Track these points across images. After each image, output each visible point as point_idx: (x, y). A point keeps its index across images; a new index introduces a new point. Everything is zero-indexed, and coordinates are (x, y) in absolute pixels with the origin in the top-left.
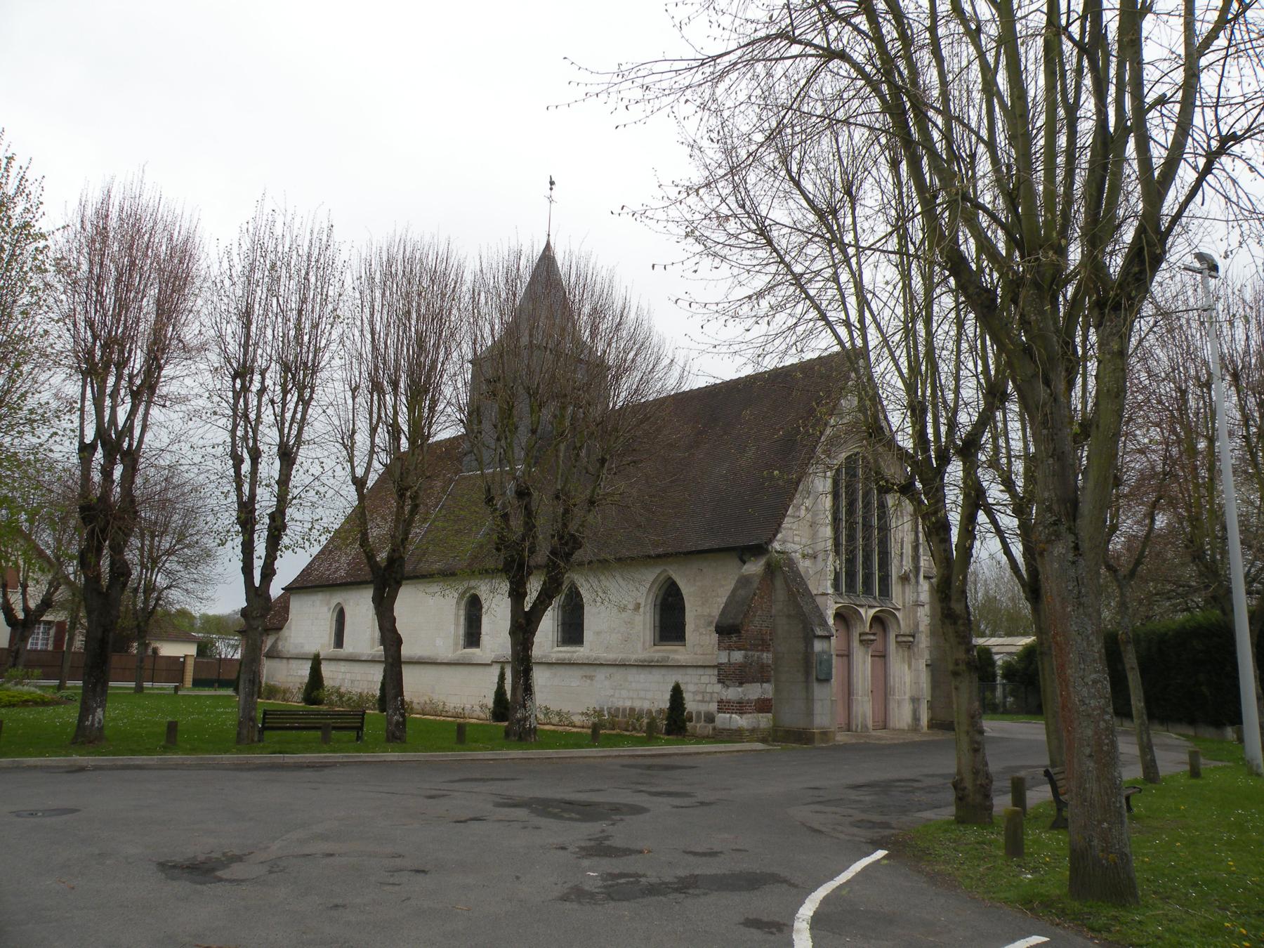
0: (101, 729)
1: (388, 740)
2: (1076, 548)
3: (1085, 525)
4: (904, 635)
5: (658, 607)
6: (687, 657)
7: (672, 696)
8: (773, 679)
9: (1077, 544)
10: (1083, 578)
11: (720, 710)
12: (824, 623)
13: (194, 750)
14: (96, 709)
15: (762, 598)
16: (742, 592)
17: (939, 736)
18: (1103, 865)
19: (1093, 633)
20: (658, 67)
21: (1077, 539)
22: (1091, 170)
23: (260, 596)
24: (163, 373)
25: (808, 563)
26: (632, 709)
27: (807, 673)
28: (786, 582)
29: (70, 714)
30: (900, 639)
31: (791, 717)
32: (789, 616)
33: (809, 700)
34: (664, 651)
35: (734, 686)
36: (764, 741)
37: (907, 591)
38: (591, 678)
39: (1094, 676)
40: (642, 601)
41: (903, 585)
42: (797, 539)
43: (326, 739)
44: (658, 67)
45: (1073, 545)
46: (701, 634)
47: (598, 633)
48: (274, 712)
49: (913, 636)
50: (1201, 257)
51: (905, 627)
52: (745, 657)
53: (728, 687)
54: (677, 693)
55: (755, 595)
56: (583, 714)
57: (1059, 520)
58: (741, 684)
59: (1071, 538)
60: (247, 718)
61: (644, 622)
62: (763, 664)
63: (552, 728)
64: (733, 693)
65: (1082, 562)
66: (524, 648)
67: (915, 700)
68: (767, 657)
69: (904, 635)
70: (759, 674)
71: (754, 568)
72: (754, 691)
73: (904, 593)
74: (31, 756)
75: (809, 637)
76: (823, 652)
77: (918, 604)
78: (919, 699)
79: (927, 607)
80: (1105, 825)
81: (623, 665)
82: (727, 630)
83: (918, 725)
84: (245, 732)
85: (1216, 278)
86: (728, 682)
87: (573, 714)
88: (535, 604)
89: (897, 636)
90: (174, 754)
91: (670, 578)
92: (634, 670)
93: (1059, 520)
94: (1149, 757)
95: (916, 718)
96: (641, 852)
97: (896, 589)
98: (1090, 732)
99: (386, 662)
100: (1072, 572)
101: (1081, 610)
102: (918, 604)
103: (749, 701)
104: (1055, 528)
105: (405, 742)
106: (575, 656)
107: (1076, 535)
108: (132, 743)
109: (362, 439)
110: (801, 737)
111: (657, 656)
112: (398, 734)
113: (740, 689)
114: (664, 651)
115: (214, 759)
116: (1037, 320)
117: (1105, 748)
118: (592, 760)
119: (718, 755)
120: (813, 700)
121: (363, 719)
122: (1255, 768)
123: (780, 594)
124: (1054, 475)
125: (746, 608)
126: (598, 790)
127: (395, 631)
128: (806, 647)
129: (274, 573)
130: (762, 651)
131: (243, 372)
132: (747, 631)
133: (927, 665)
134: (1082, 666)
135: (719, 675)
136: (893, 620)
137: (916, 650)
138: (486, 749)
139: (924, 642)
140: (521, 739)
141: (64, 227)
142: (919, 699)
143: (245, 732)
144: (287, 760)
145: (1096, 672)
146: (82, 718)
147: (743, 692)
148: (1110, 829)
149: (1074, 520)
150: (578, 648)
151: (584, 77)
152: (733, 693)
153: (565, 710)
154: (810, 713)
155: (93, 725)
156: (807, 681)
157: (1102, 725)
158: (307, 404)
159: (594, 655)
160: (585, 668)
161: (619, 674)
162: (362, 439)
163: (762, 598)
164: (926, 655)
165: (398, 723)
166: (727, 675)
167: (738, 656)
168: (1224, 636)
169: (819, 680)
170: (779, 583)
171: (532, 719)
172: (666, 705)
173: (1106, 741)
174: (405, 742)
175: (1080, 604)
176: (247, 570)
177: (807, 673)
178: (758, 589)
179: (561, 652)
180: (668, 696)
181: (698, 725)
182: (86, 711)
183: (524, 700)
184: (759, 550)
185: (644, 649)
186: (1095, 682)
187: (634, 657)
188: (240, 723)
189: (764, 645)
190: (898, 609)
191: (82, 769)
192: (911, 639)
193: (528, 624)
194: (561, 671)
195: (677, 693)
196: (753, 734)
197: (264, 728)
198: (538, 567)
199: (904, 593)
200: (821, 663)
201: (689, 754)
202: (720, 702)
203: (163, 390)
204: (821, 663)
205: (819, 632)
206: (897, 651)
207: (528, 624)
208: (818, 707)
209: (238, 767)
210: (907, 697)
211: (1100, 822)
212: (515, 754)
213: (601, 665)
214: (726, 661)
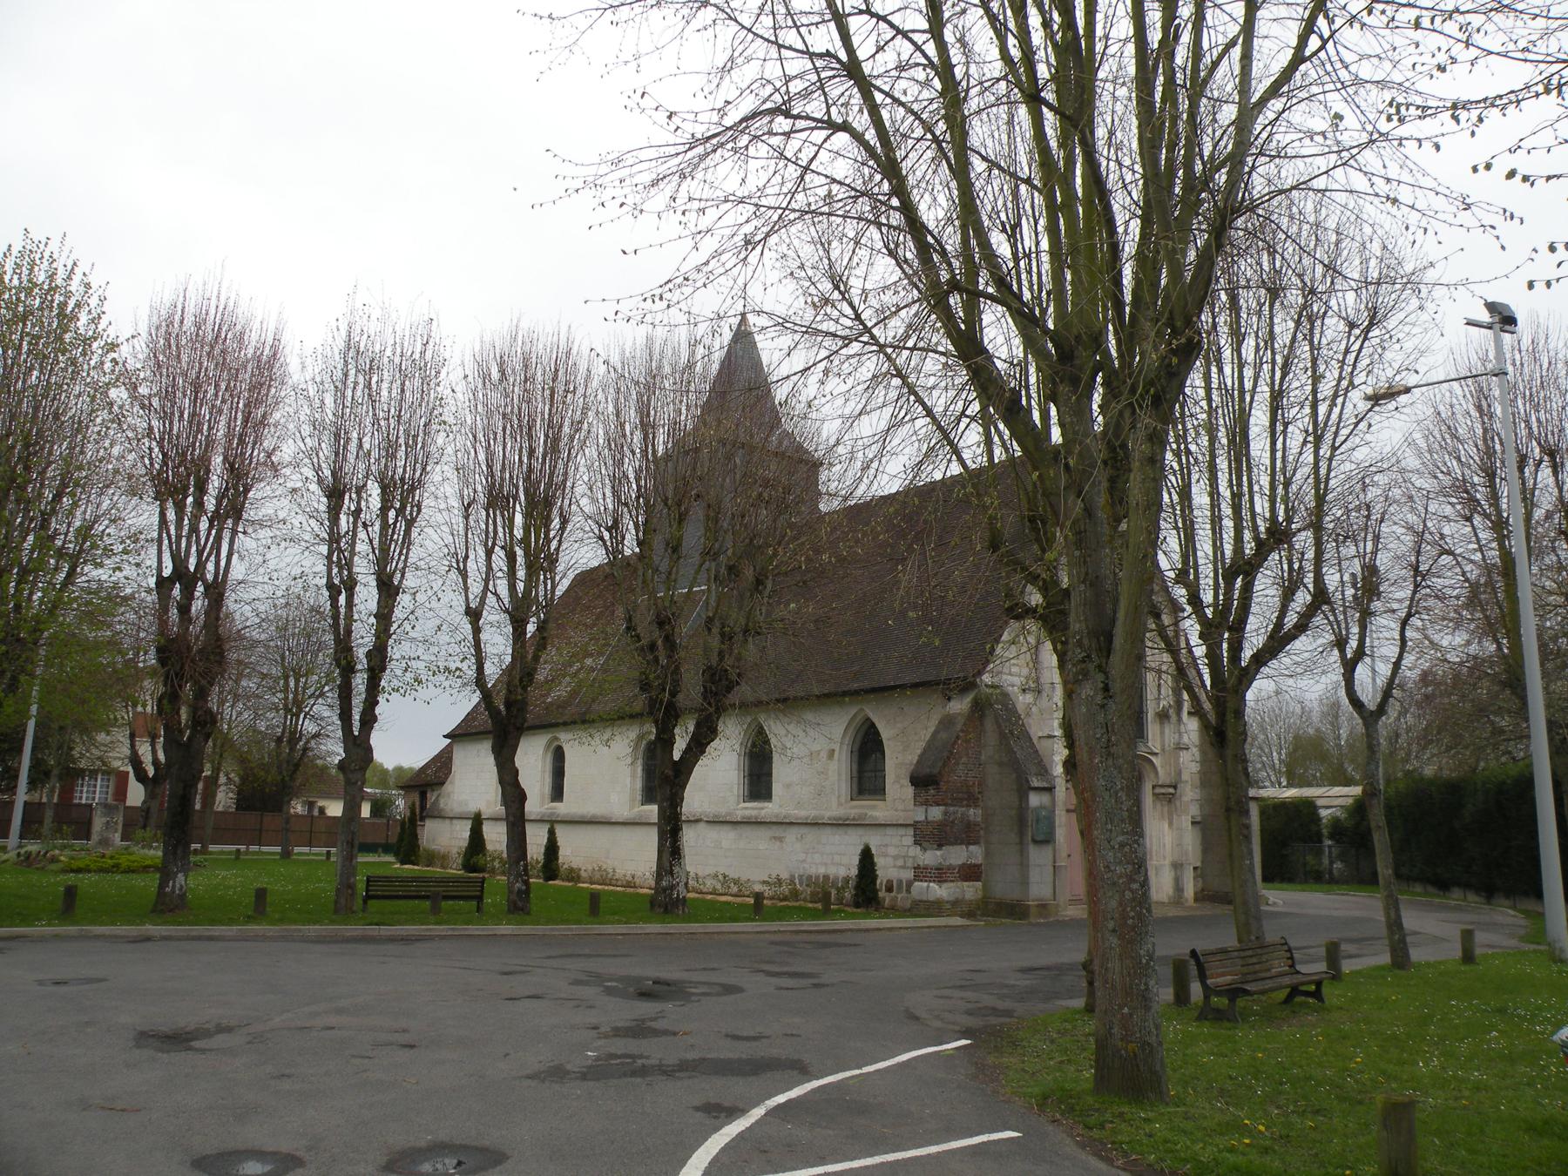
0: (183, 896)
1: (510, 911)
2: (1106, 689)
3: (1117, 662)
4: (1162, 786)
5: (856, 754)
6: (886, 813)
7: (860, 861)
8: (982, 841)
9: (1107, 685)
10: (1113, 724)
11: (917, 878)
12: (1044, 771)
13: (281, 921)
14: (177, 873)
15: (968, 741)
16: (943, 735)
17: (1208, 909)
18: (1121, 1056)
19: (1122, 789)
20: (644, 155)
21: (1107, 678)
22: (1052, 262)
23: (359, 745)
24: (251, 495)
25: (1029, 698)
26: (826, 877)
27: (1021, 834)
28: (997, 722)
29: (151, 882)
30: (1158, 790)
31: (1004, 888)
32: (1001, 764)
33: (1024, 866)
34: (862, 807)
35: (932, 849)
36: (970, 915)
37: (1167, 731)
38: (780, 839)
39: (1120, 838)
40: (837, 747)
41: (1162, 723)
42: (1014, 669)
43: (435, 910)
44: (644, 155)
45: (1102, 685)
46: (902, 786)
47: (788, 786)
48: (379, 879)
49: (1175, 787)
50: (1492, 307)
51: (1163, 775)
52: (945, 813)
53: (925, 850)
54: (867, 857)
55: (958, 738)
56: (764, 882)
57: (1088, 656)
58: (940, 846)
59: (1100, 677)
60: (346, 887)
61: (839, 771)
62: (969, 822)
63: (729, 898)
64: (931, 857)
65: (1112, 706)
66: (671, 804)
67: (1177, 866)
68: (974, 814)
69: (1162, 786)
70: (967, 834)
71: (960, 706)
72: (957, 855)
73: (1162, 733)
74: (102, 924)
75: (1024, 789)
76: (1042, 807)
77: (1180, 747)
78: (1182, 865)
79: (1195, 750)
80: (1126, 1010)
81: (815, 824)
82: (922, 781)
83: (1180, 897)
84: (343, 901)
85: (1513, 333)
86: (924, 844)
87: (754, 882)
88: (685, 752)
89: (1154, 787)
90: (259, 924)
91: (868, 719)
92: (828, 830)
93: (1088, 656)
94: (1397, 937)
95: (1179, 889)
96: (675, 1034)
97: (1152, 729)
98: (1114, 904)
99: (507, 819)
100: (1101, 718)
101: (1110, 762)
102: (1180, 747)
103: (950, 867)
104: (1083, 666)
105: (528, 913)
106: (763, 812)
107: (1106, 673)
108: (219, 911)
109: (475, 566)
110: (1014, 910)
111: (853, 812)
112: (520, 904)
113: (938, 853)
114: (862, 807)
115: (300, 930)
116: (1072, 422)
117: (1130, 922)
118: (732, 936)
119: (902, 931)
120: (1028, 866)
121: (482, 887)
122: (1557, 952)
123: (991, 737)
124: (1085, 605)
125: (945, 754)
126: (713, 969)
127: (517, 785)
128: (1021, 801)
129: (375, 719)
130: (968, 806)
131: (335, 494)
132: (948, 782)
133: (1193, 823)
134: (1109, 827)
135: (915, 836)
136: (1148, 767)
137: (1178, 803)
138: (619, 922)
139: (1190, 794)
140: (666, 911)
141: (133, 337)
142: (1182, 865)
143: (343, 901)
144: (382, 933)
145: (1124, 833)
146: (162, 886)
147: (942, 856)
148: (1131, 1015)
149: (1108, 657)
150: (766, 804)
151: (569, 170)
152: (931, 857)
153: (744, 878)
154: (1025, 882)
155: (173, 891)
156: (1021, 843)
157: (1128, 895)
158: (410, 524)
159: (784, 811)
160: (774, 827)
161: (811, 835)
162: (475, 566)
163: (968, 741)
164: (1194, 810)
165: (520, 891)
166: (927, 835)
167: (936, 813)
168: (1526, 784)
169: (1035, 842)
170: (989, 724)
171: (681, 888)
172: (854, 872)
173: (1132, 914)
174: (528, 913)
175: (1109, 754)
176: (345, 716)
177: (1021, 834)
178: (962, 731)
179: (746, 808)
180: (856, 860)
181: (900, 896)
182: (165, 872)
183: (671, 865)
184: (968, 686)
185: (840, 804)
186: (1122, 845)
187: (828, 814)
188: (338, 890)
189: (971, 799)
190: (1156, 754)
191: (148, 939)
192: (1171, 790)
193: (676, 776)
194: (748, 831)
195: (867, 857)
196: (956, 906)
197: (368, 897)
198: (691, 710)
199: (1162, 733)
200: (1038, 821)
201: (867, 930)
202: (917, 868)
203: (250, 513)
204: (1038, 821)
205: (1035, 783)
206: (1154, 808)
207: (676, 776)
208: (1034, 875)
209: (320, 940)
210: (1167, 862)
211: (1121, 1007)
212: (654, 928)
213: (791, 824)
214: (923, 818)
